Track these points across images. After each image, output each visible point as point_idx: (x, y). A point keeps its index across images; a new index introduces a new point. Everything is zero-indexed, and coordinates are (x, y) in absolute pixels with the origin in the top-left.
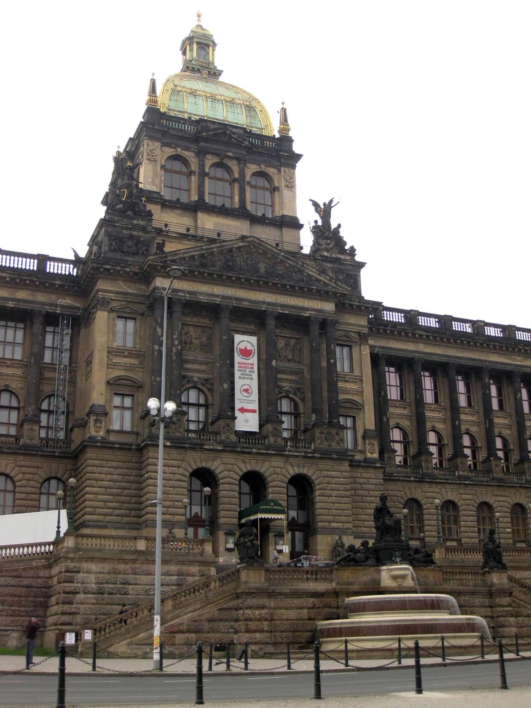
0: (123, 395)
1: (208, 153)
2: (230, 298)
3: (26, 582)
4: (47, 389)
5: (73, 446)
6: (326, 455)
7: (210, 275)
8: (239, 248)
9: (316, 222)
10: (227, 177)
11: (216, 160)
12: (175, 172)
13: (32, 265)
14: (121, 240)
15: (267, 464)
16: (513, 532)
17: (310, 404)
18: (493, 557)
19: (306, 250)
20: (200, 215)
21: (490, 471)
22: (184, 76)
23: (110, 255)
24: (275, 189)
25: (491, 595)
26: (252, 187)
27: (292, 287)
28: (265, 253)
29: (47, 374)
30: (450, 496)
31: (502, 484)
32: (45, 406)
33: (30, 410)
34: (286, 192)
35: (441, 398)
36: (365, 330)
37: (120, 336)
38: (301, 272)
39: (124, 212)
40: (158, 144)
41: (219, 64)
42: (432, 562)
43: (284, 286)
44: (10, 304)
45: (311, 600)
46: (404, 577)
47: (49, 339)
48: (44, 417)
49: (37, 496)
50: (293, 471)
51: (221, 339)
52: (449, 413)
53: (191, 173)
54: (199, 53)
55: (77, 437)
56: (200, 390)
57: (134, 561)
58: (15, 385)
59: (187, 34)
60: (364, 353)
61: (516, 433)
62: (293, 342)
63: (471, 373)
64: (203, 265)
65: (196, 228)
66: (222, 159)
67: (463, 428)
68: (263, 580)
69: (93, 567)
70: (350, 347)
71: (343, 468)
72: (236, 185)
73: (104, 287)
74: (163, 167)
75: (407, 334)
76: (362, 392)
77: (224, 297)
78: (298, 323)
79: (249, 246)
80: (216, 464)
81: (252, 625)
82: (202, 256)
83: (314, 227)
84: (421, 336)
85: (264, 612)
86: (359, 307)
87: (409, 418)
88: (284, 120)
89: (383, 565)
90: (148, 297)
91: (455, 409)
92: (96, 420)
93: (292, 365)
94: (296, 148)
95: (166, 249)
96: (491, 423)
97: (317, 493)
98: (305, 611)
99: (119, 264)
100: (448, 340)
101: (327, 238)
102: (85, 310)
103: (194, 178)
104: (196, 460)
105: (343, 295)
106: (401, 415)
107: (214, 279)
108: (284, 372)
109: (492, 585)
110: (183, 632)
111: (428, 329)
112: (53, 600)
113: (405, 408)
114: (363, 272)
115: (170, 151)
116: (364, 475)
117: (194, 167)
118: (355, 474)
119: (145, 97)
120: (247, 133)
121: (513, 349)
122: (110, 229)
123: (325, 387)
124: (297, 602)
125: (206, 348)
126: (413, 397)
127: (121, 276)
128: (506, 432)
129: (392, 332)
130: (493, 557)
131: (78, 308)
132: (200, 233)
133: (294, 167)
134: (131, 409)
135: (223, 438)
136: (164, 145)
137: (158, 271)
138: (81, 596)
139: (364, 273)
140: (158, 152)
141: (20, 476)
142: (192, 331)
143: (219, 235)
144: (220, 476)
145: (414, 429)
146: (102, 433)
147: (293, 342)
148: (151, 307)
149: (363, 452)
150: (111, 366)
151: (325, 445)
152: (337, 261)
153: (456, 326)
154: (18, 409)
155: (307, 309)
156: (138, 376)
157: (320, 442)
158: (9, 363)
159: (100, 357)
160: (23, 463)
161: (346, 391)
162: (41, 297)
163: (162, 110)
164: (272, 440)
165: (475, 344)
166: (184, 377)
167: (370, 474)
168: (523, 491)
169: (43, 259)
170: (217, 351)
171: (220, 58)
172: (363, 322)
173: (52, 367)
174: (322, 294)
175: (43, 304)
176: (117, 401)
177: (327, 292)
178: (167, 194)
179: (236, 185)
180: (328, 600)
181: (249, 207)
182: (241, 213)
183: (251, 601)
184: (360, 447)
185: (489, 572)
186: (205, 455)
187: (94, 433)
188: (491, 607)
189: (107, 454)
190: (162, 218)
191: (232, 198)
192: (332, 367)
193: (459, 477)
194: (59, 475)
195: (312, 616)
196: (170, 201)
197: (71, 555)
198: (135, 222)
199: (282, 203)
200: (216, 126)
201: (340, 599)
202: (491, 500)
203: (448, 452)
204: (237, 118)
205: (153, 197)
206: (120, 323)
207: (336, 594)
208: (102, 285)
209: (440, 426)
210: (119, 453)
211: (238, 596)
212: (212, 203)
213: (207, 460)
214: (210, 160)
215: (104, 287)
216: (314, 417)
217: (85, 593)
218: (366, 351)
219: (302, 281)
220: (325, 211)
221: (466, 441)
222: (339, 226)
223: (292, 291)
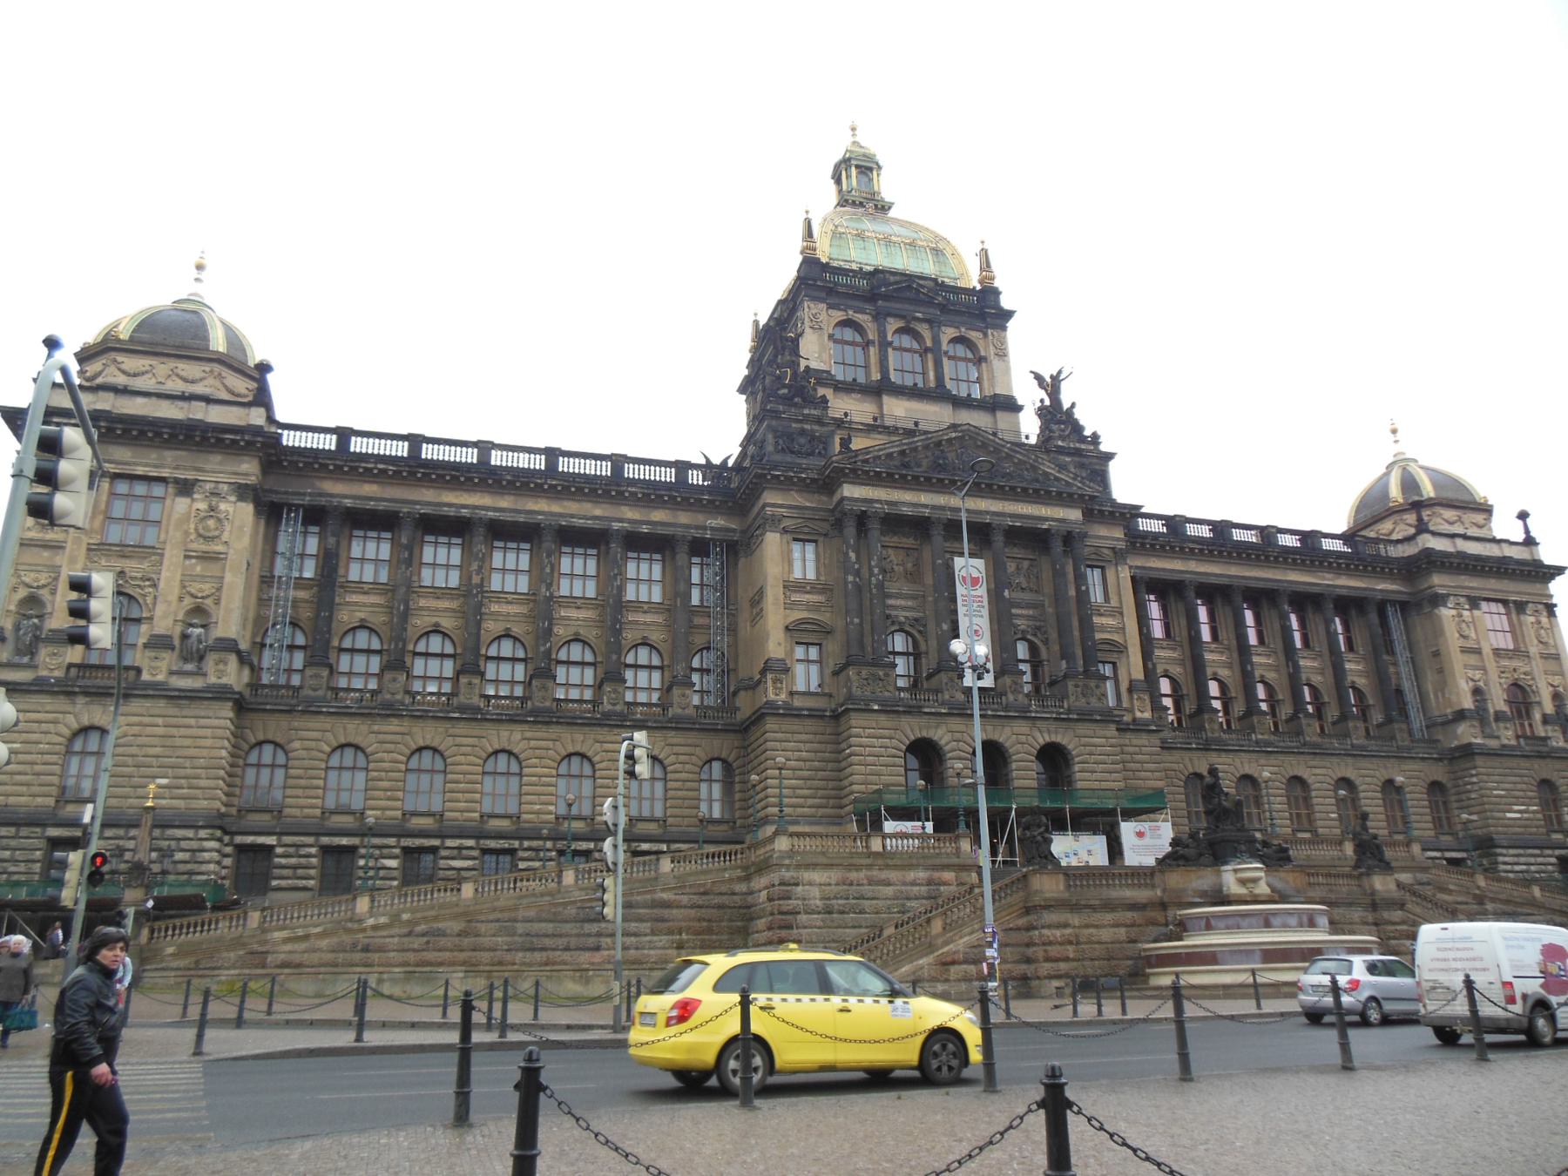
0: (807, 644)
1: (889, 315)
2: (943, 508)
3: (717, 900)
4: (699, 640)
5: (740, 716)
6: (1085, 717)
7: (915, 478)
8: (950, 440)
9: (1042, 401)
10: (916, 346)
11: (901, 324)
12: (847, 343)
13: (669, 475)
14: (790, 437)
15: (1007, 731)
16: (1340, 818)
17: (1057, 648)
18: (1370, 854)
19: (1033, 440)
20: (886, 399)
21: (1299, 733)
22: (844, 213)
23: (778, 457)
24: (980, 360)
25: (1374, 906)
26: (950, 358)
27: (1025, 490)
28: (984, 446)
29: (698, 621)
30: (1247, 770)
31: (1317, 751)
32: (696, 663)
33: (680, 669)
34: (996, 363)
35: (1222, 635)
36: (1121, 545)
37: (797, 566)
38: (1035, 469)
39: (792, 399)
40: (823, 306)
41: (887, 195)
42: (1289, 859)
43: (1013, 488)
44: (645, 529)
45: (1129, 914)
46: (1255, 881)
47: (695, 572)
49: (695, 785)
50: (1042, 739)
51: (934, 563)
52: (1235, 655)
53: (867, 344)
54: (857, 178)
55: (745, 705)
56: (908, 633)
57: (870, 867)
58: (656, 637)
59: (839, 156)
60: (1123, 575)
61: (1331, 680)
62: (1026, 564)
63: (1261, 597)
64: (905, 466)
65: (882, 416)
66: (908, 322)
67: (1257, 674)
68: (1062, 887)
69: (817, 876)
70: (1103, 568)
71: (1108, 733)
72: (930, 356)
74: (831, 337)
75: (1172, 548)
76: (1123, 629)
77: (934, 507)
78: (1033, 538)
79: (962, 438)
80: (940, 732)
81: (1054, 951)
82: (902, 453)
83: (1040, 409)
84: (1192, 550)
85: (1068, 931)
86: (1112, 513)
87: (1182, 663)
88: (986, 265)
89: (1226, 863)
90: (832, 511)
91: (1243, 649)
92: (775, 681)
93: (1027, 596)
94: (1006, 302)
95: (853, 446)
96: (1297, 667)
97: (1076, 768)
98: (1123, 930)
99: (791, 469)
100: (1230, 554)
101: (1059, 422)
102: (743, 532)
103: (873, 351)
104: (914, 728)
105: (1092, 498)
106: (1169, 658)
107: (920, 484)
108: (1019, 606)
109: (1373, 893)
110: (960, 963)
111: (1199, 540)
112: (761, 923)
113: (1174, 649)
114: (1111, 463)
115: (839, 315)
116: (1135, 742)
117: (872, 335)
118: (1122, 741)
119: (798, 244)
120: (939, 286)
121: (1321, 563)
122: (774, 423)
123: (1075, 623)
124: (1109, 917)
125: (914, 576)
126: (1185, 633)
127: (794, 484)
128: (1317, 679)
129: (1152, 546)
130: (1370, 854)
131: (734, 531)
132: (888, 422)
133: (1004, 328)
134: (820, 662)
135: (947, 697)
136: (830, 307)
137: (846, 475)
138: (803, 918)
139: (1114, 468)
140: (823, 316)
141: (672, 758)
143: (916, 424)
144: (947, 748)
145: (1190, 678)
146: (783, 696)
147: (1026, 564)
148: (838, 525)
149: (1131, 710)
150: (790, 606)
151: (1082, 702)
152: (1078, 453)
153: (1238, 535)
154: (661, 668)
155: (1046, 519)
156: (825, 617)
157: (1075, 700)
158: (646, 607)
159: (773, 595)
160: (675, 741)
161: (1103, 628)
162: (684, 518)
163: (824, 260)
164: (1011, 697)
165: (1267, 557)
166: (888, 617)
167: (1143, 739)
168: (1350, 760)
169: (682, 467)
170: (929, 580)
171: (887, 186)
172: (1119, 533)
173: (702, 610)
175: (687, 526)
176: (800, 652)
177: (1071, 495)
178: (839, 373)
179: (930, 356)
180: (1153, 914)
181: (949, 385)
182: (939, 394)
183: (1050, 917)
184: (1125, 705)
185: (1368, 875)
186: (924, 720)
187: (772, 696)
188: (1376, 924)
189: (796, 725)
190: (840, 405)
191: (924, 374)
192: (1083, 597)
193: (1257, 742)
194: (723, 756)
195: (1133, 936)
196: (843, 382)
197: (787, 862)
198: (806, 411)
199: (992, 378)
200: (898, 278)
201: (1170, 913)
202: (1305, 773)
203: (1238, 708)
204: (924, 266)
205: (824, 378)
206: (796, 548)
207: (1163, 906)
208: (771, 497)
209: (1224, 673)
210: (809, 722)
211: (1027, 911)
212: (899, 382)
213: (928, 728)
214: (893, 325)
215: (772, 499)
216: (1064, 664)
217: (807, 913)
218: (1125, 574)
219: (1037, 481)
220: (1052, 386)
221: (1261, 692)
222: (1073, 405)
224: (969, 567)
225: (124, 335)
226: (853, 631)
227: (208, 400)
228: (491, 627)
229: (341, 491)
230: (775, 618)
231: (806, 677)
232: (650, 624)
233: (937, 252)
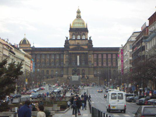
6: (86, 67)
34: (86, 36)
48: (61, 64)
73: (64, 52)
78: (84, 53)
88: (87, 25)
115: (72, 33)
142: (73, 55)
156: (68, 61)
159: (64, 59)
162: (60, 52)
172: (92, 52)
174: (87, 51)
214: (77, 33)
218: (93, 55)
220: (90, 38)
223: (83, 51)
224: (78, 57)
225: (21, 43)
226: (70, 61)
227: (27, 48)
228: (47, 61)
229: (36, 53)
230: (64, 61)
231: (67, 65)
232: (57, 60)
233: (83, 24)
